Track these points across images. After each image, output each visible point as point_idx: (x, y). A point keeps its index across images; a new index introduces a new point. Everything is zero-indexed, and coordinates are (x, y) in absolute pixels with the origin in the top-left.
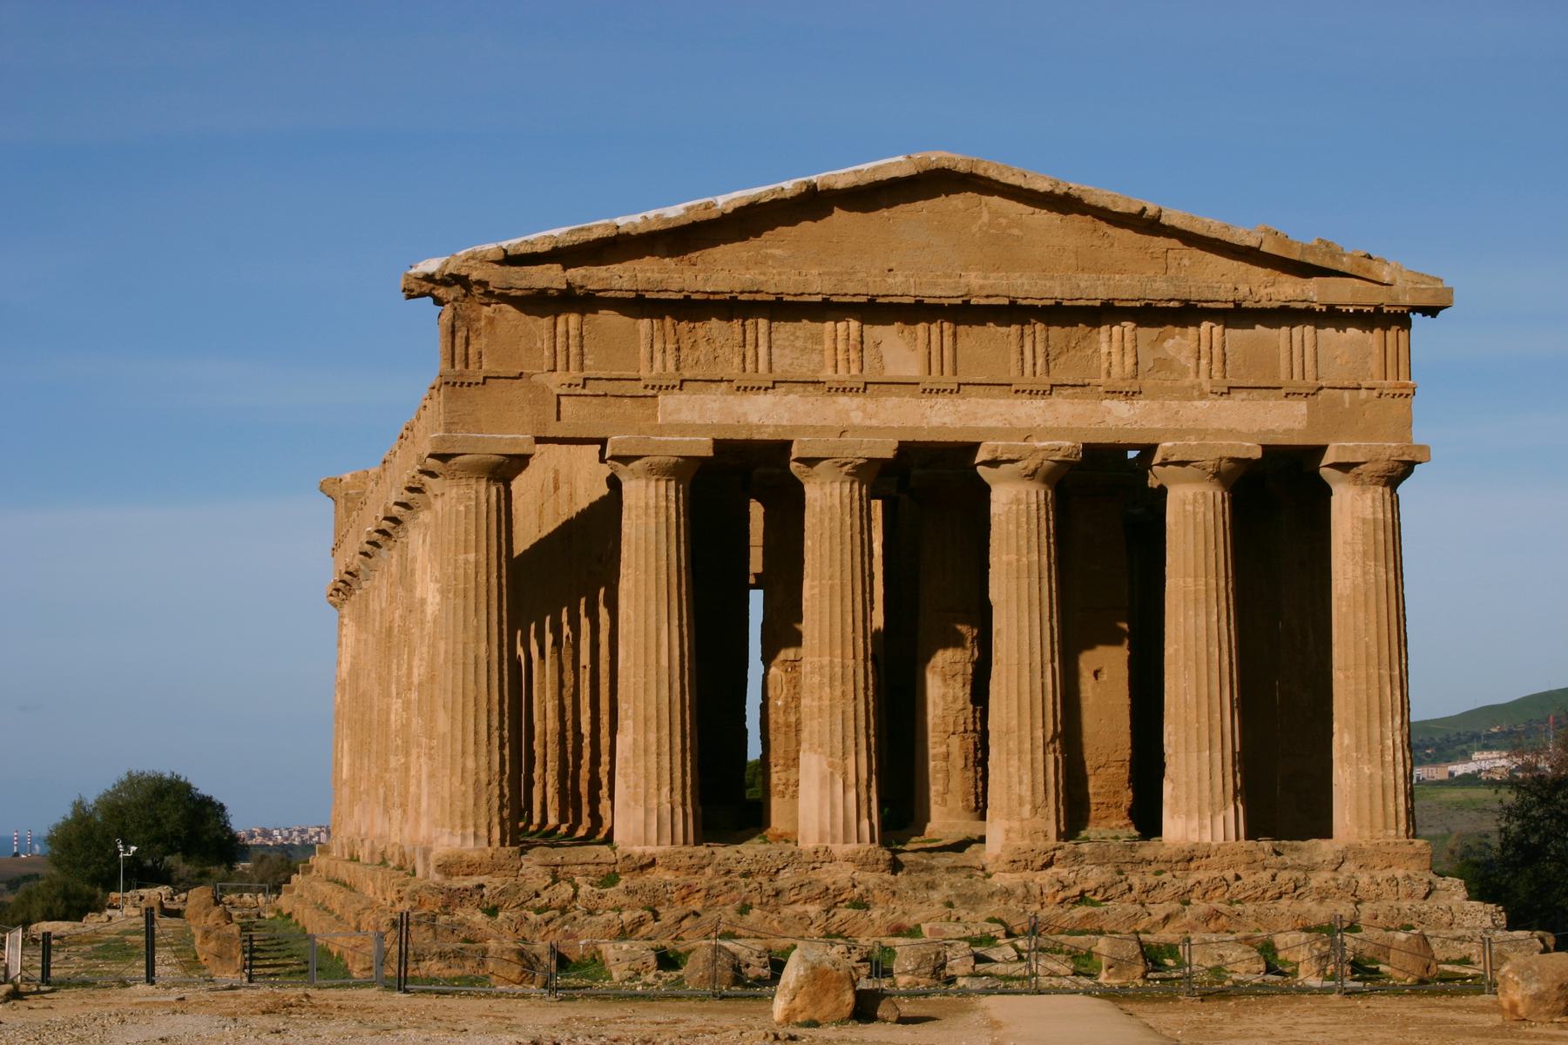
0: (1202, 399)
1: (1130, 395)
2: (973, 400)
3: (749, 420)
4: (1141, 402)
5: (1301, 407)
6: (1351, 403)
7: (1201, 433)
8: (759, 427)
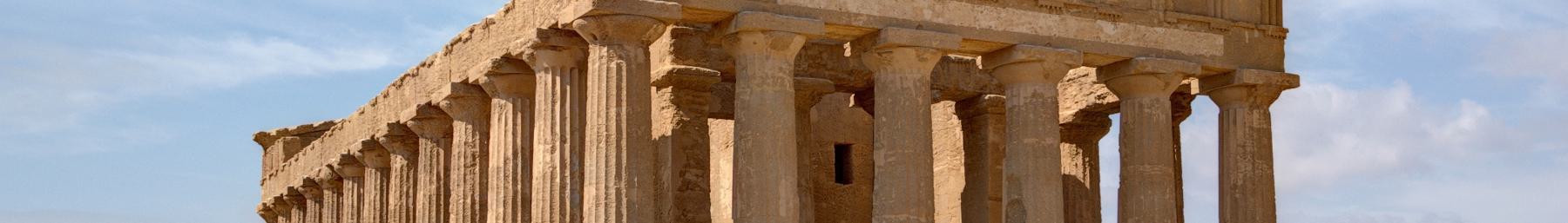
0: (1161, 26)
1: (1114, 18)
2: (1010, 9)
3: (849, 9)
4: (1122, 24)
5: (1220, 40)
6: (1249, 39)
7: (1159, 54)
8: (857, 15)
